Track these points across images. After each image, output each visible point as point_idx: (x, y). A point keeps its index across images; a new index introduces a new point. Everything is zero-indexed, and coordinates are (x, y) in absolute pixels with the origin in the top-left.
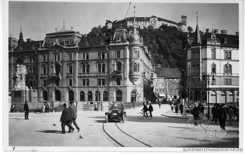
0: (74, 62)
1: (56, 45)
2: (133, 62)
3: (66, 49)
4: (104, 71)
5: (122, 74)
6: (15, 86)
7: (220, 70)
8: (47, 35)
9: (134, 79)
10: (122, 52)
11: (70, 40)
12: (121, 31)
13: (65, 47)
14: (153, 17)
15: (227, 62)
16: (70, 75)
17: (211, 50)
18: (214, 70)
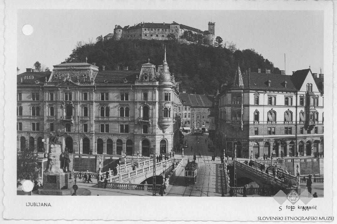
0: (91, 102)
1: (67, 81)
3: (80, 87)
6: (49, 170)
7: (263, 118)
8: (54, 66)
9: (164, 126)
10: (150, 94)
11: (85, 75)
12: (149, 68)
13: (78, 85)
14: (175, 23)
15: (272, 108)
16: (86, 119)
17: (254, 94)
18: (257, 117)
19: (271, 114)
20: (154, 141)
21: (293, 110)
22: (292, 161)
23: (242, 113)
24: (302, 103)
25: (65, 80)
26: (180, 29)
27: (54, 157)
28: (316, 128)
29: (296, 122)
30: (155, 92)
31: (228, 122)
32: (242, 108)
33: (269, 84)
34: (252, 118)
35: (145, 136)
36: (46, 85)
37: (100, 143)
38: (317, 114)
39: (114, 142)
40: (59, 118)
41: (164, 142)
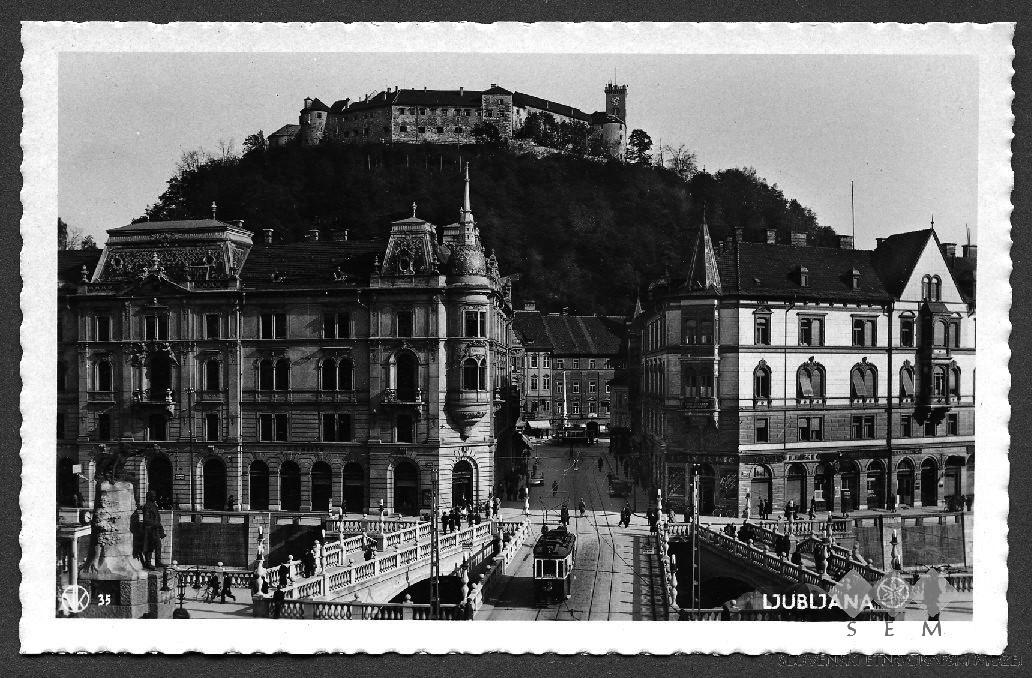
1: (152, 278)
2: (463, 353)
5: (419, 399)
7: (783, 388)
8: (111, 233)
9: (464, 416)
10: (418, 316)
11: (210, 260)
12: (417, 232)
14: (496, 90)
19: (809, 376)
20: (433, 468)
21: (879, 360)
22: (875, 524)
23: (716, 373)
24: (906, 338)
25: (146, 274)
26: (515, 108)
27: (113, 520)
28: (954, 417)
29: (890, 398)
30: (436, 311)
31: (672, 403)
32: (717, 357)
33: (803, 279)
34: (746, 390)
35: (403, 452)
36: (83, 291)
38: (957, 371)
39: (303, 471)
40: (128, 396)
41: (464, 470)
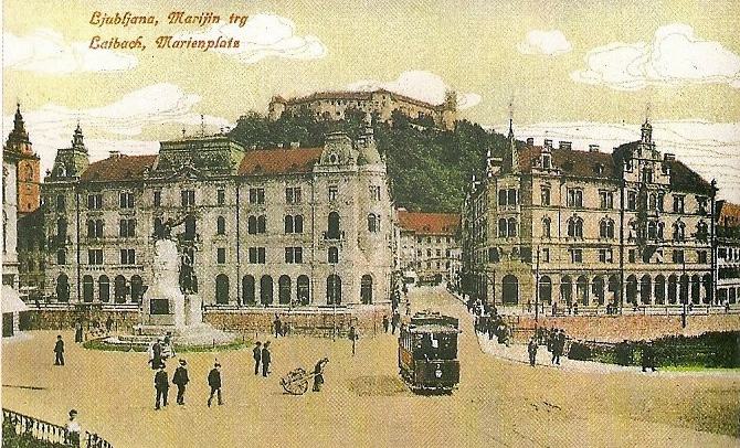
4: (299, 230)
37: (248, 281)
38: (662, 225)
